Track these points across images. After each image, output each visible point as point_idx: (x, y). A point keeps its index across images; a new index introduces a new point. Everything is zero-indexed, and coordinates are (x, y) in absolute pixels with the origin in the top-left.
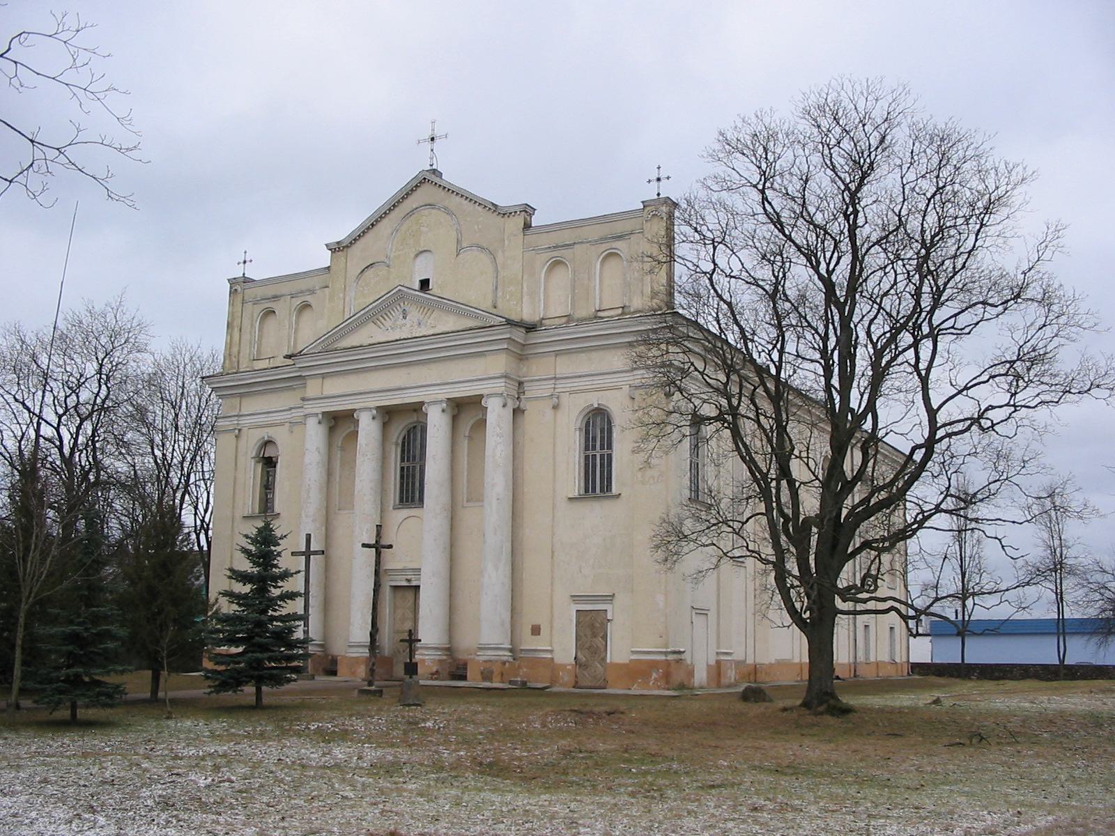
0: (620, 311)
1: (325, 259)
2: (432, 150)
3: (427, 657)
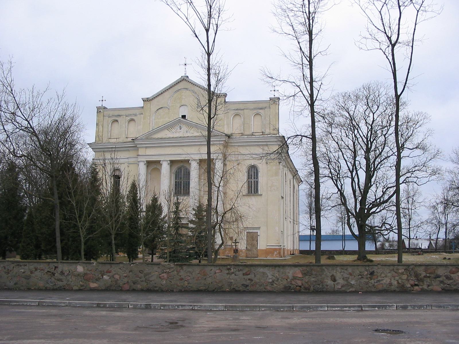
0: (261, 134)
1: (141, 104)
2: (185, 69)
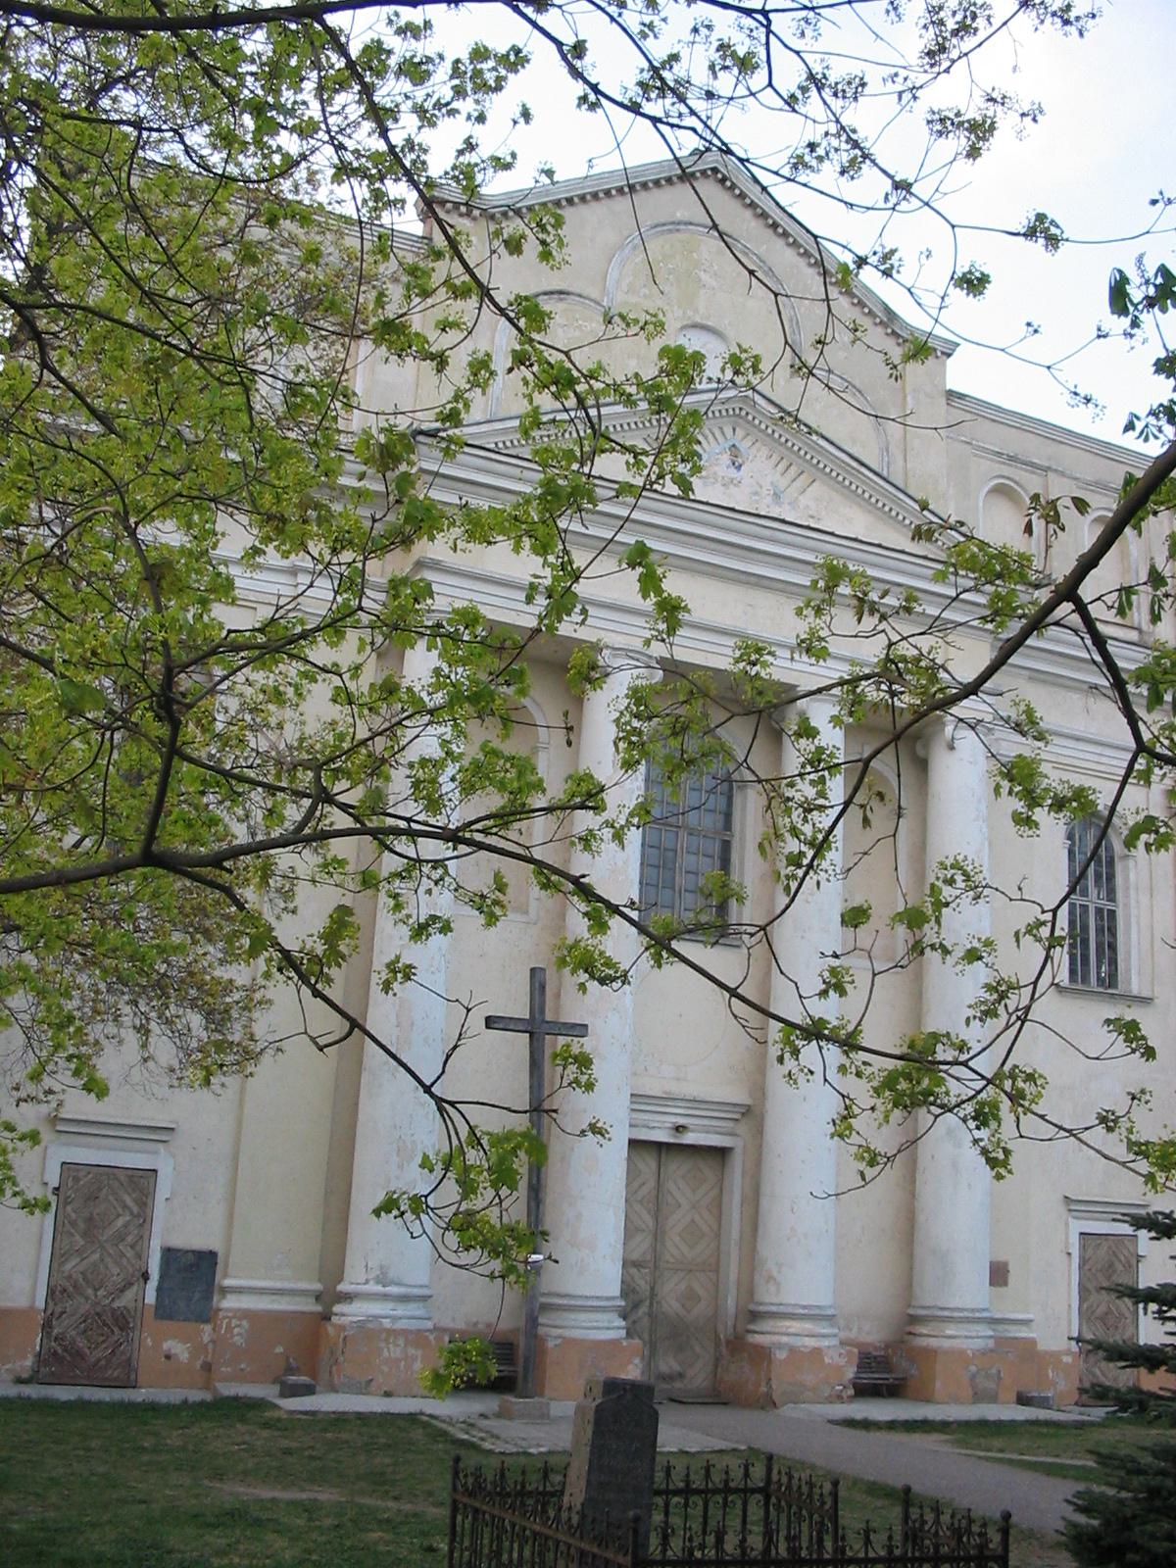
3: (826, 1343)
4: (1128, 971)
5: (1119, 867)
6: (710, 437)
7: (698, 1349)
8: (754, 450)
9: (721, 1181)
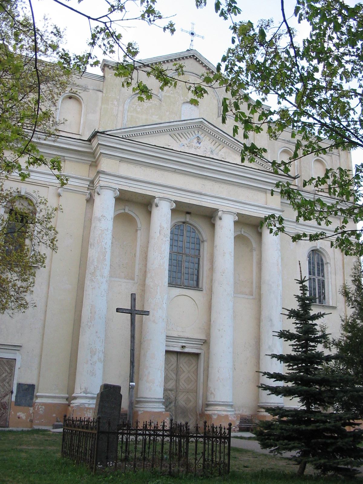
3: (229, 413)
4: (329, 298)
5: (325, 267)
6: (191, 134)
7: (190, 417)
8: (204, 138)
9: (197, 364)
